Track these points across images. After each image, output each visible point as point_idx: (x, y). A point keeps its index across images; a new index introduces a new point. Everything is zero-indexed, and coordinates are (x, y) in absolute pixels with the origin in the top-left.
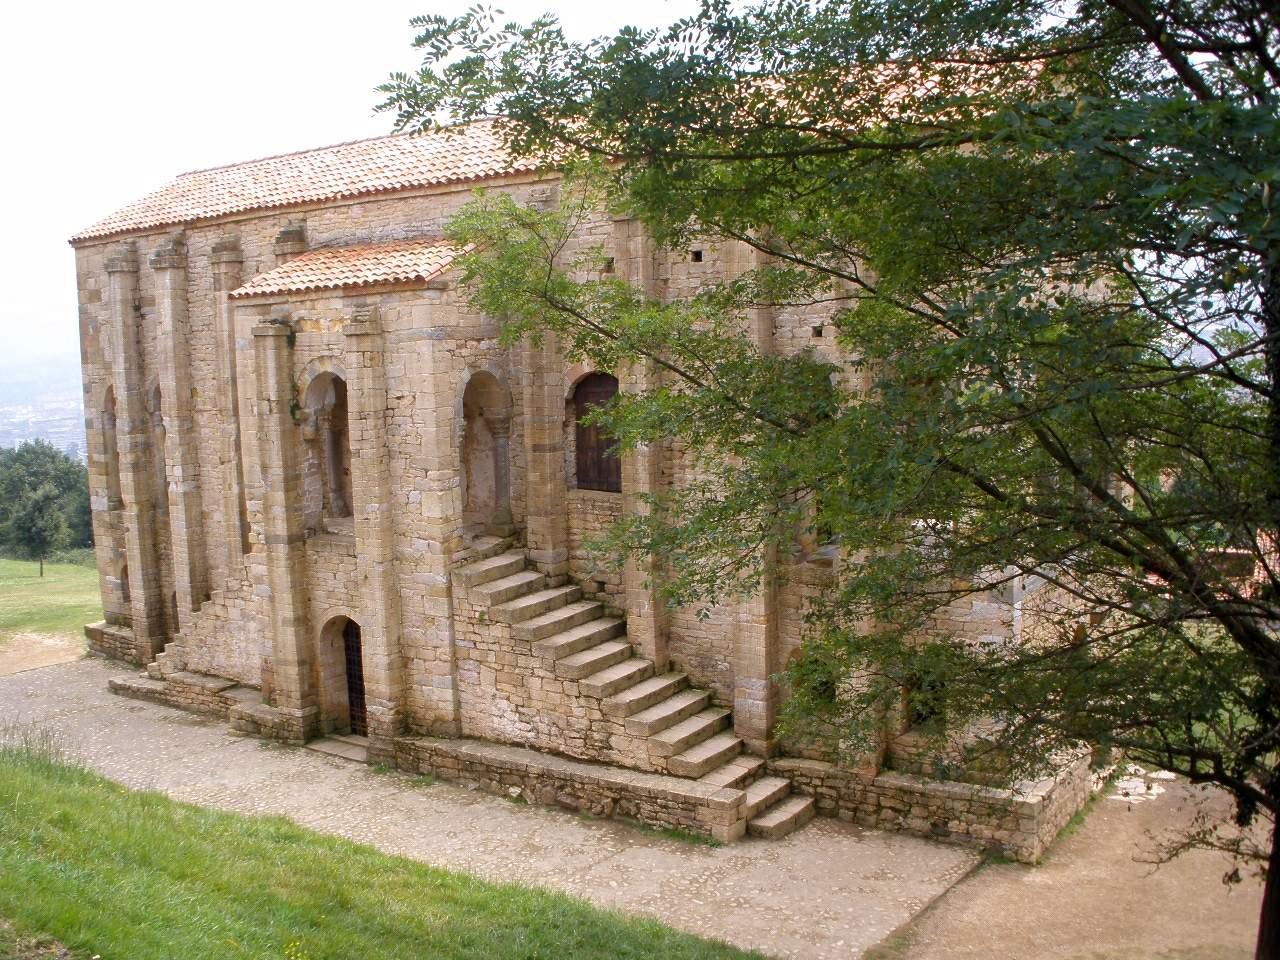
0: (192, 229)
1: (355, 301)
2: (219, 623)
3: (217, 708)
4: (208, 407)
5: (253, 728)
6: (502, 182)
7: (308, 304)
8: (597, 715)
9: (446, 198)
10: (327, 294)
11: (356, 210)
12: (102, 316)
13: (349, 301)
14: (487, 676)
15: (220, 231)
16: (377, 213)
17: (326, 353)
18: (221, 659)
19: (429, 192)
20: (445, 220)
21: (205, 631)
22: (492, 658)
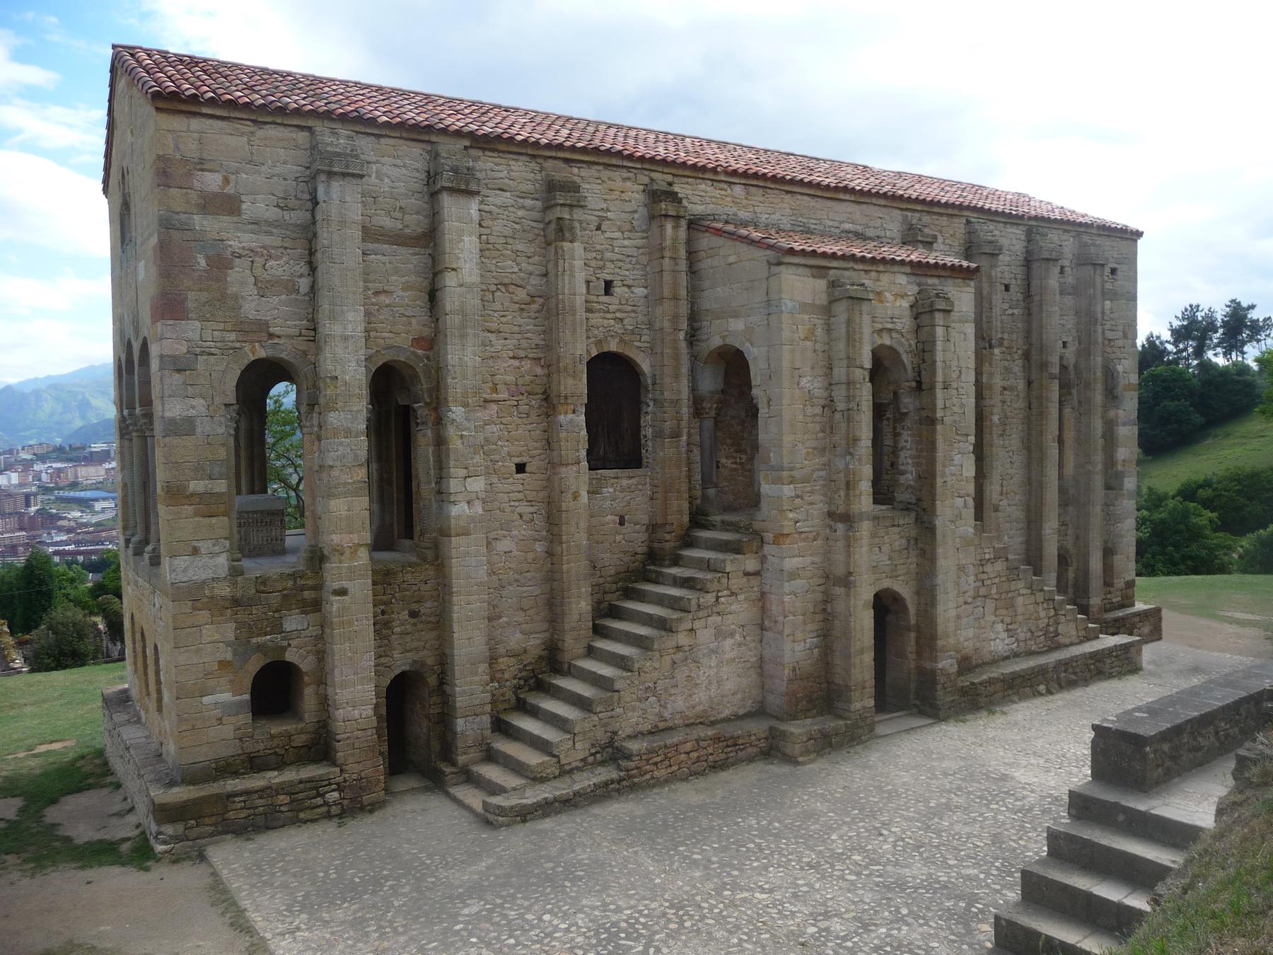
0: (484, 149)
1: (918, 279)
2: (679, 656)
3: (724, 756)
4: (501, 396)
5: (826, 745)
6: (882, 202)
7: (873, 274)
8: (1052, 612)
9: (830, 203)
10: (896, 268)
11: (738, 190)
12: (240, 240)
13: (913, 279)
14: (990, 605)
15: (533, 165)
16: (762, 199)
17: (890, 326)
18: (678, 703)
19: (819, 193)
20: (831, 223)
21: (656, 675)
22: (994, 591)
